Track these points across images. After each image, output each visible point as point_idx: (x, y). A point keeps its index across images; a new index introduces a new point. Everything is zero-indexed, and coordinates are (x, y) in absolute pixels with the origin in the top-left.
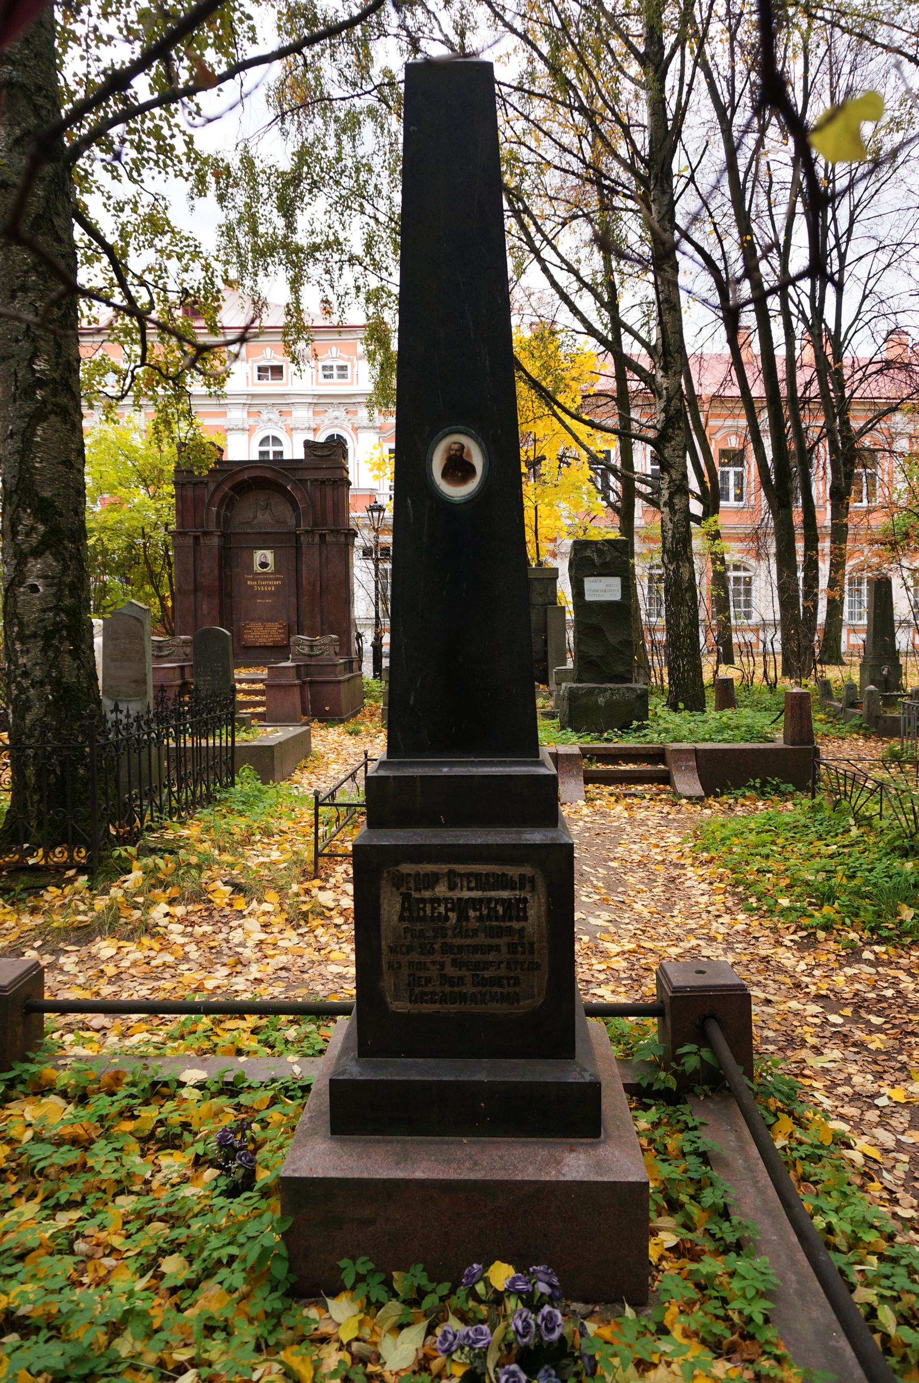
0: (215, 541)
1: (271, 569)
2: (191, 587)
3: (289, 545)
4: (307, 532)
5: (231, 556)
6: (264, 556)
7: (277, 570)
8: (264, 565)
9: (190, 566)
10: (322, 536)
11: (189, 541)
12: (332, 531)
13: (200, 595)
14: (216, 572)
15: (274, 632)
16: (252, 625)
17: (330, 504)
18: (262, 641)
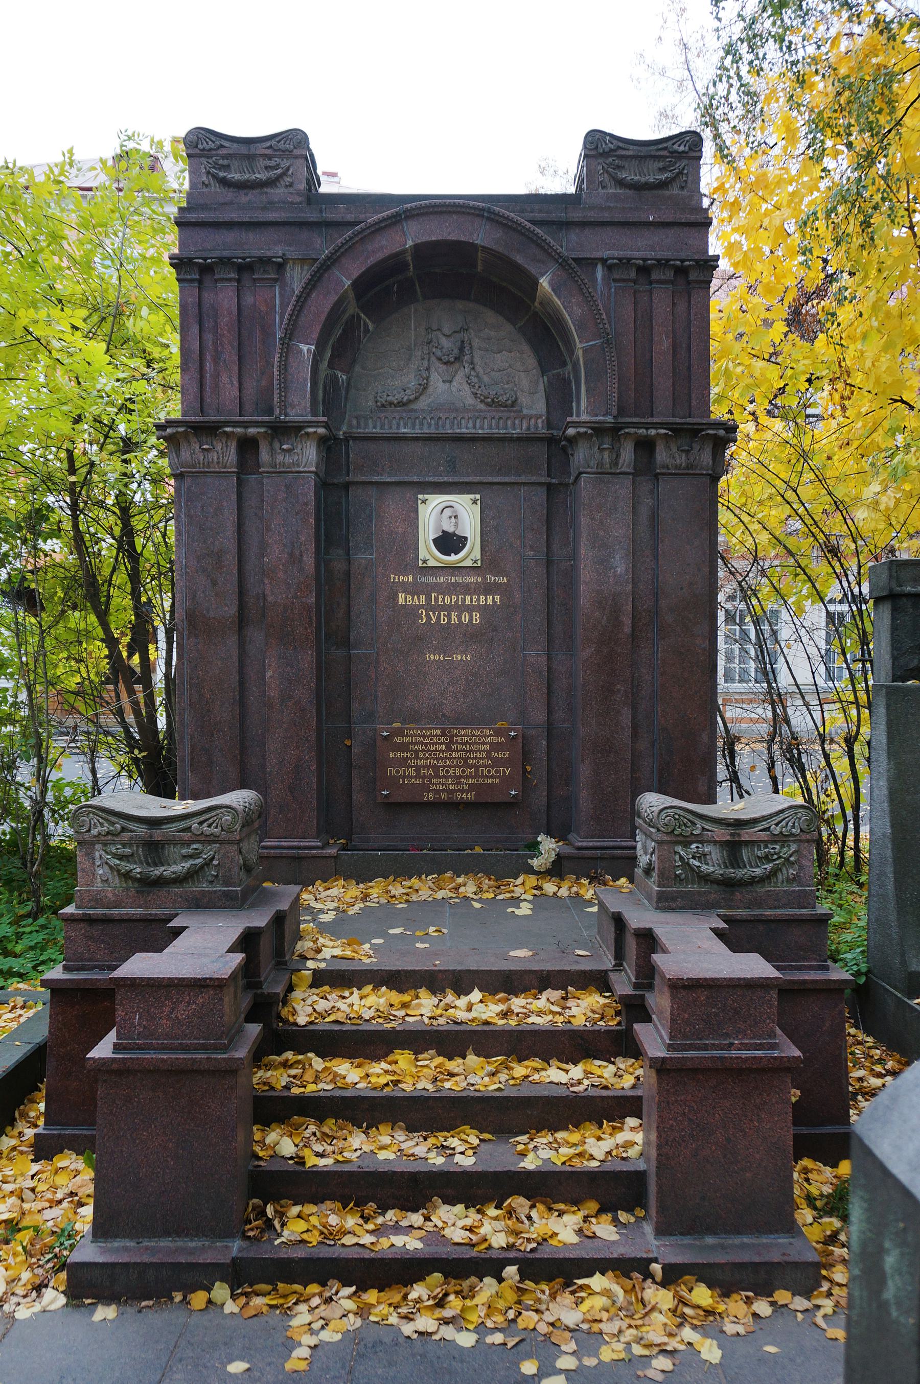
0: (308, 456)
1: (471, 554)
2: (231, 610)
3: (534, 473)
4: (599, 430)
5: (347, 506)
6: (449, 513)
7: (491, 560)
8: (449, 542)
9: (227, 540)
10: (645, 446)
11: (226, 454)
12: (677, 431)
13: (256, 636)
14: (309, 561)
15: (479, 756)
16: (413, 735)
17: (663, 344)
18: (442, 787)
